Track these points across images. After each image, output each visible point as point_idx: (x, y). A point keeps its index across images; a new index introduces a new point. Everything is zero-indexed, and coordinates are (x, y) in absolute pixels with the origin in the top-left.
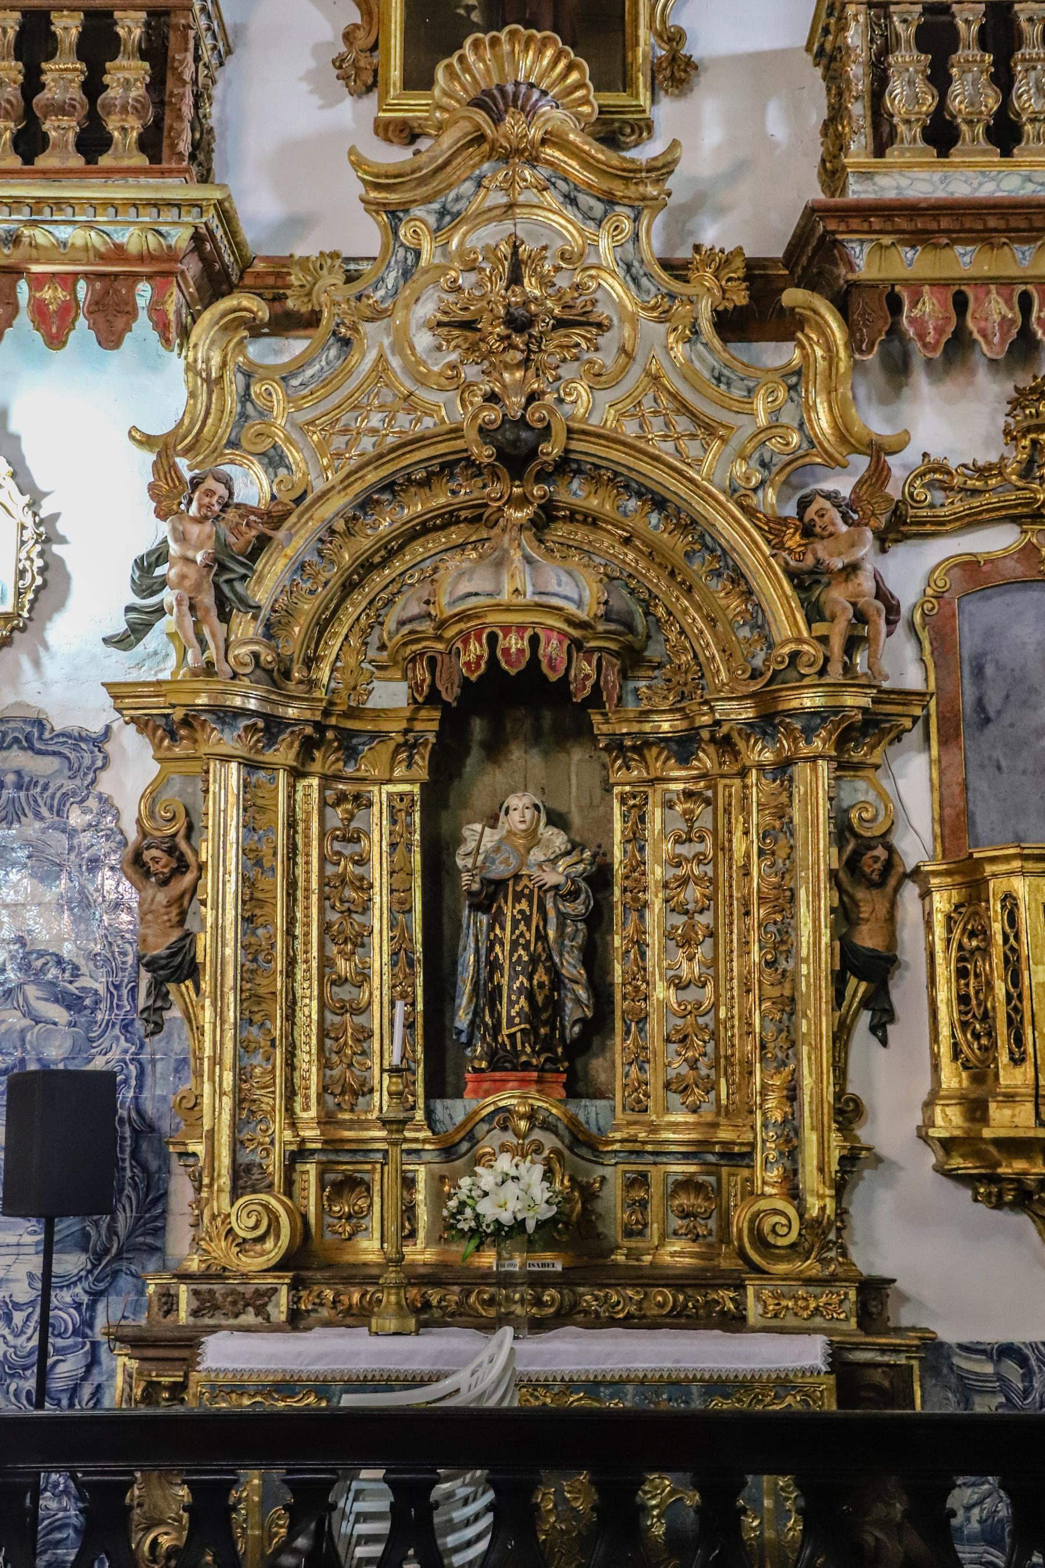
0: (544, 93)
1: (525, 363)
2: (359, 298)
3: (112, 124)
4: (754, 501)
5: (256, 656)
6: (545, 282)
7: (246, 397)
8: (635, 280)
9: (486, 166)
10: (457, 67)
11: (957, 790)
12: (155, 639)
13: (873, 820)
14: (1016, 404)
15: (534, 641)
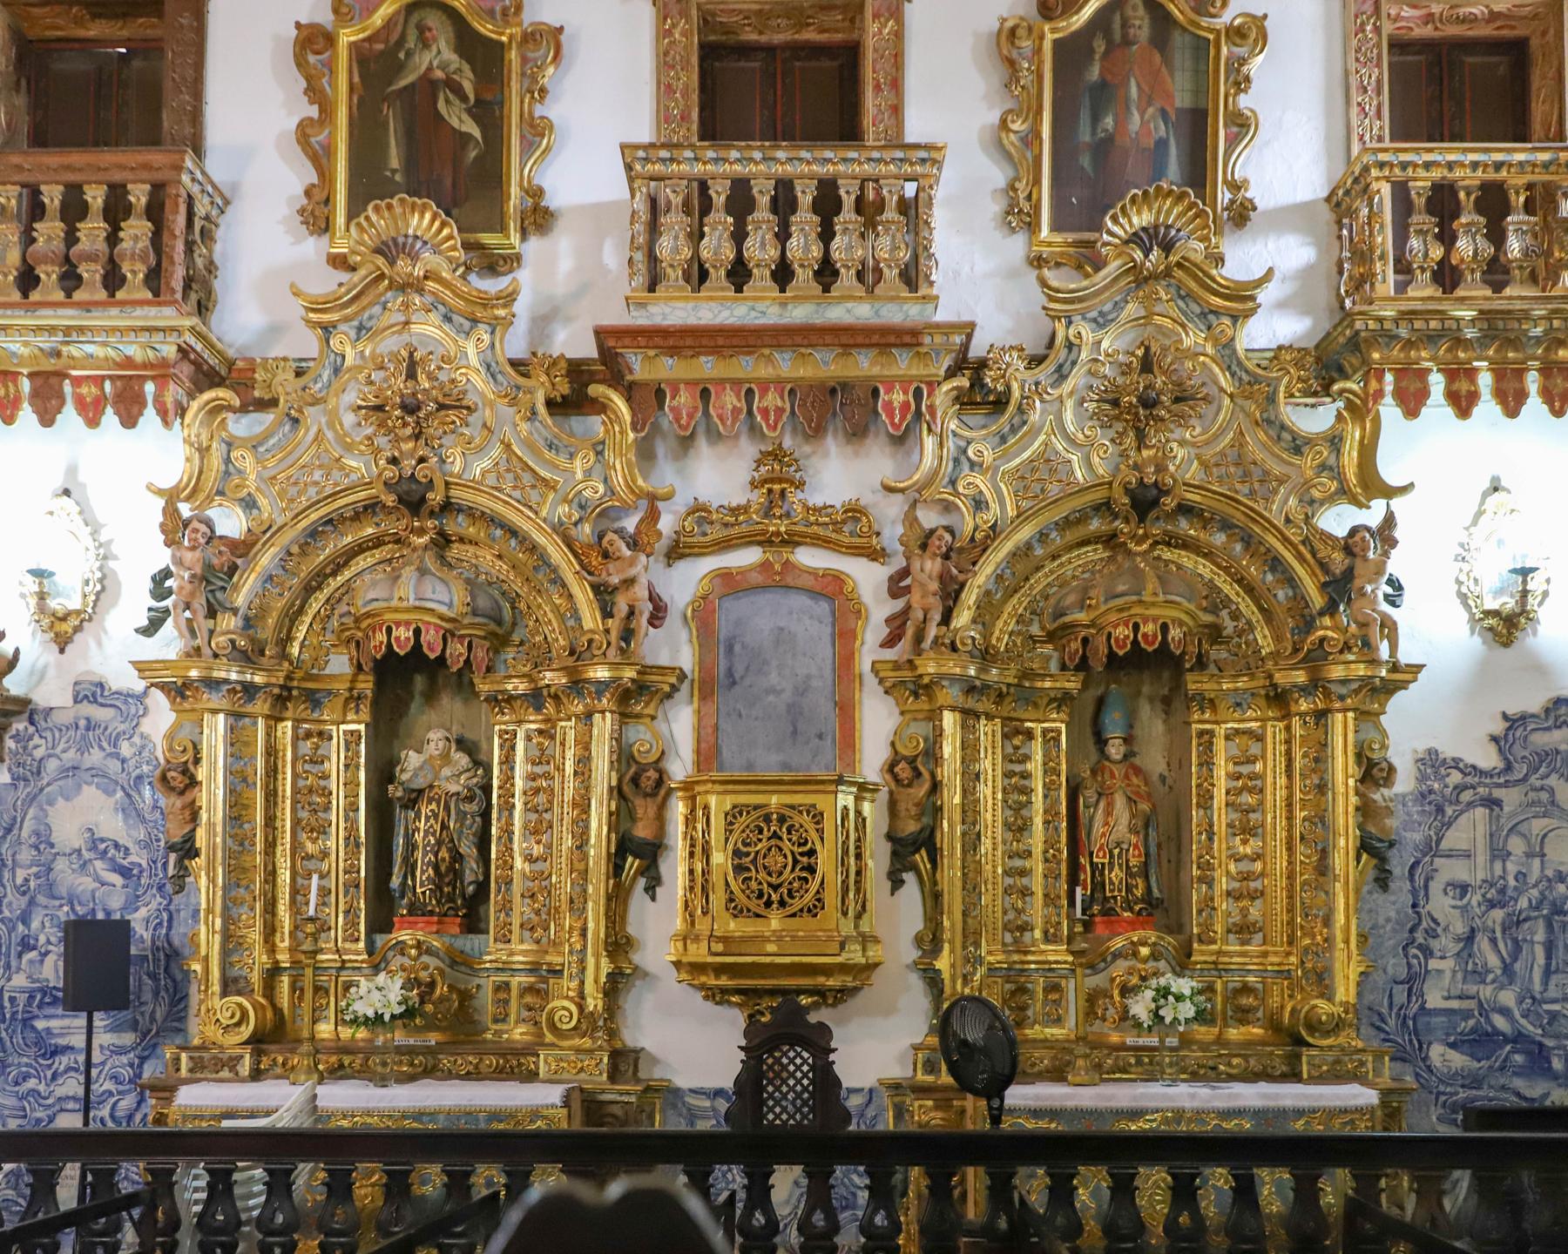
0: (425, 243)
1: (417, 437)
2: (304, 389)
3: (126, 268)
4: (573, 532)
5: (233, 642)
6: (431, 377)
7: (228, 461)
8: (493, 376)
9: (389, 294)
10: (365, 224)
11: (710, 730)
12: (169, 626)
13: (648, 752)
14: (759, 463)
15: (417, 632)
